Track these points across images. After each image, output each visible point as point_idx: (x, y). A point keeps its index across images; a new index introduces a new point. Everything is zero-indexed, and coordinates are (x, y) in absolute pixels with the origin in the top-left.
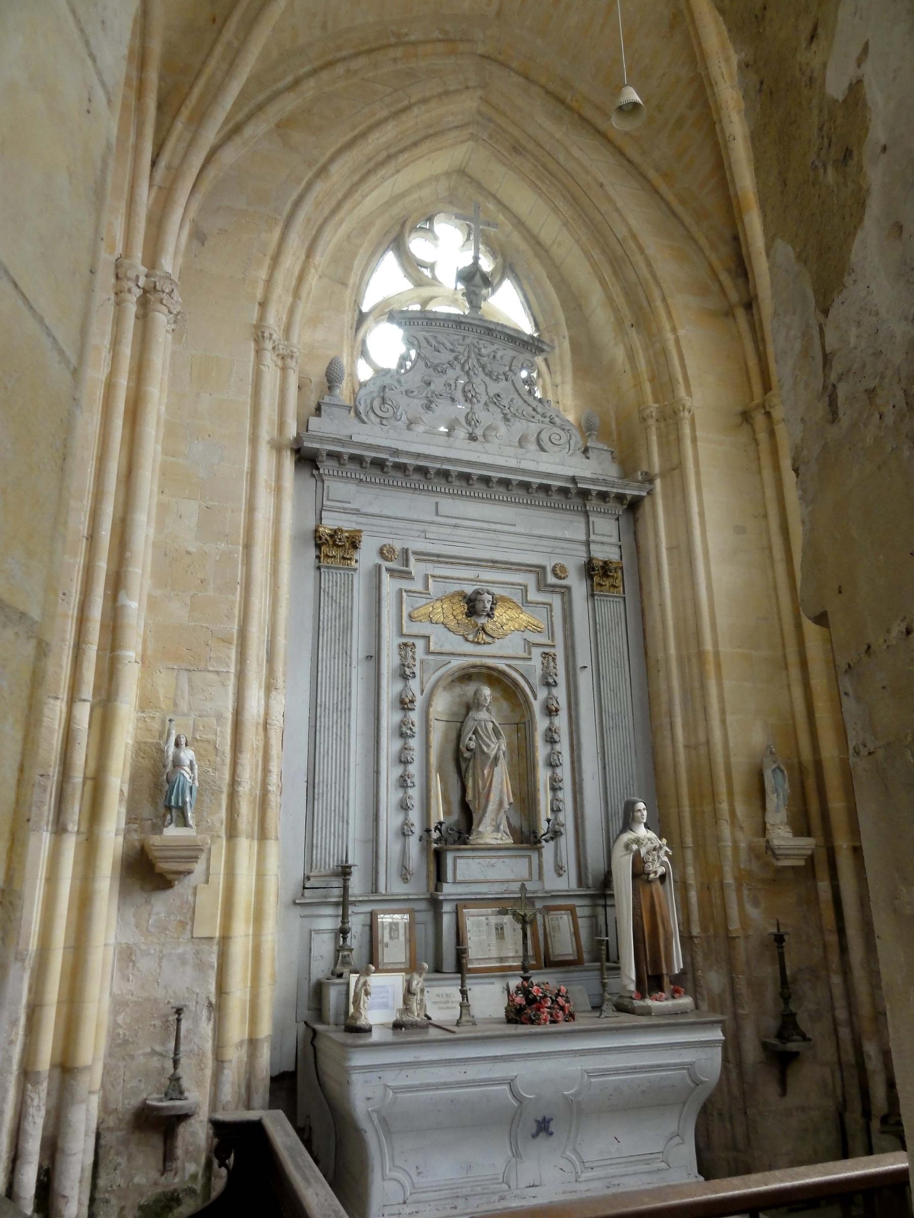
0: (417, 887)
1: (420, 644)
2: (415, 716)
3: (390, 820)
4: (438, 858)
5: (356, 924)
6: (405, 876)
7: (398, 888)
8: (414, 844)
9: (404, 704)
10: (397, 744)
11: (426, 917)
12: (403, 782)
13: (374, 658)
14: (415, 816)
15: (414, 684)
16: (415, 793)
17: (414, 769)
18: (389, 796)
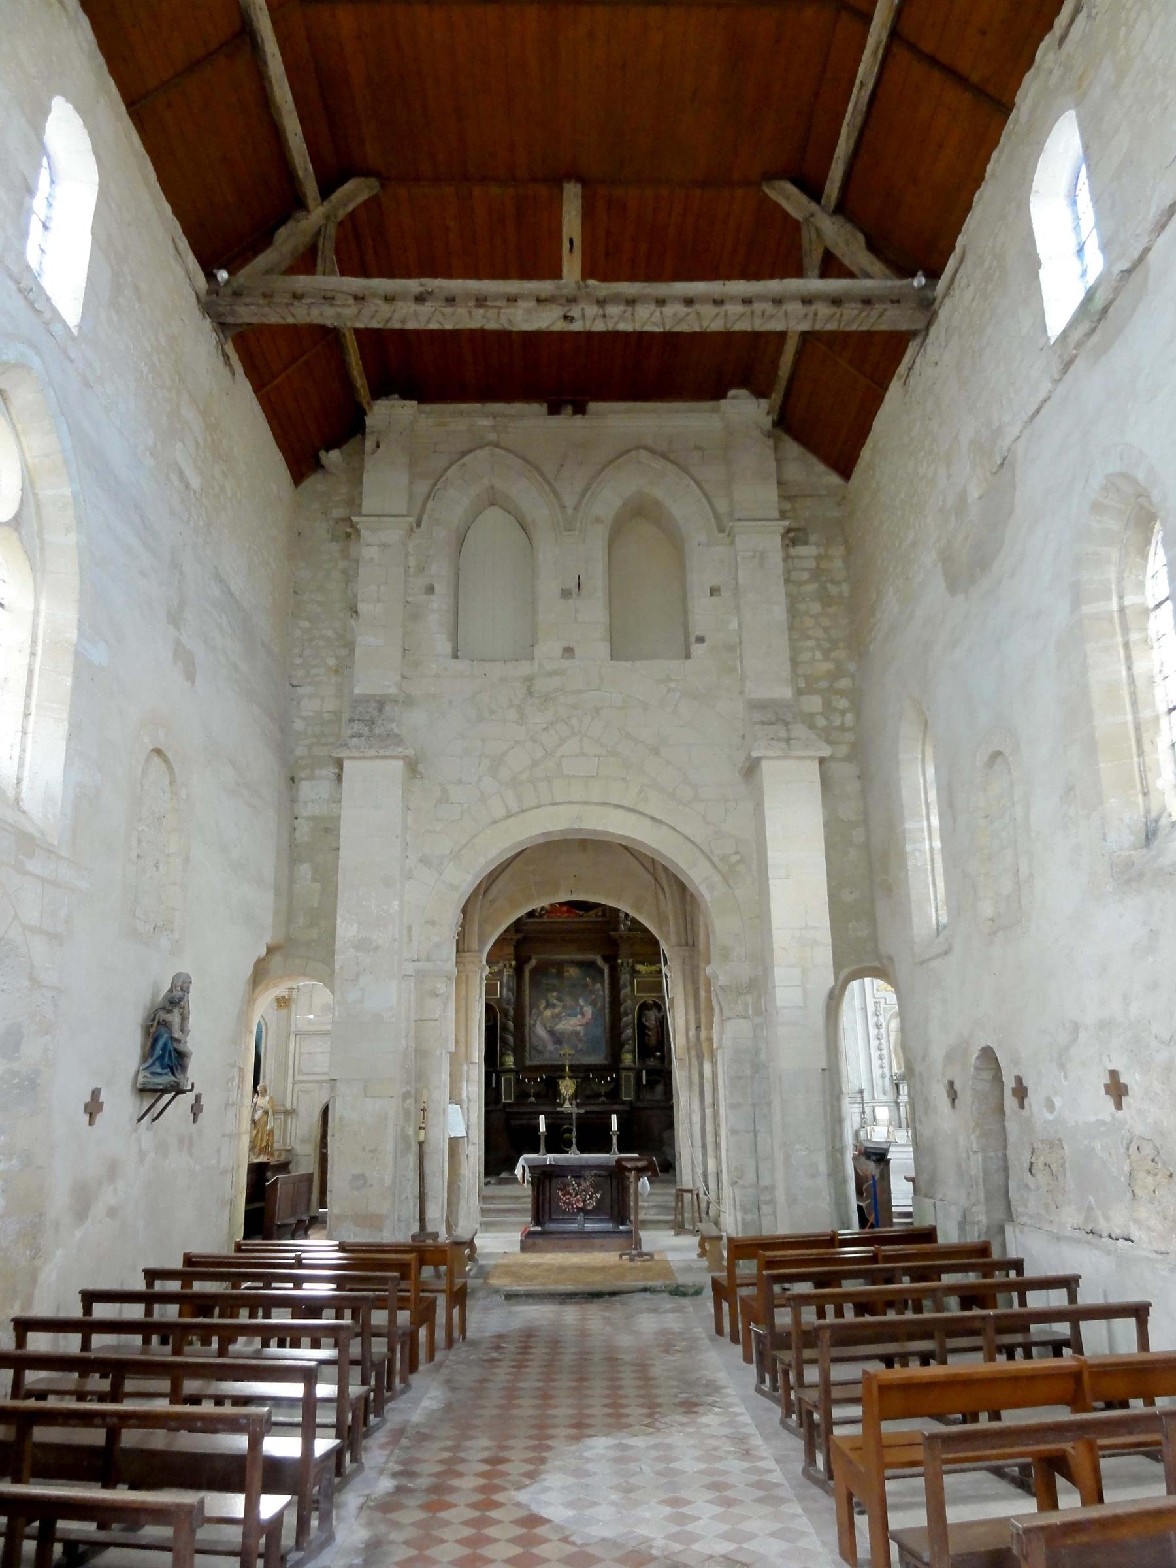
0: (891, 1096)
1: (882, 1001)
2: (883, 1031)
3: (877, 1072)
4: (897, 1085)
5: (868, 1110)
6: (885, 1093)
7: (883, 1098)
8: (887, 1079)
9: (878, 1027)
10: (877, 1042)
11: (894, 1108)
12: (881, 1058)
13: (864, 1009)
14: (886, 1070)
15: (881, 1018)
16: (885, 1061)
17: (885, 1052)
18: (876, 1063)
